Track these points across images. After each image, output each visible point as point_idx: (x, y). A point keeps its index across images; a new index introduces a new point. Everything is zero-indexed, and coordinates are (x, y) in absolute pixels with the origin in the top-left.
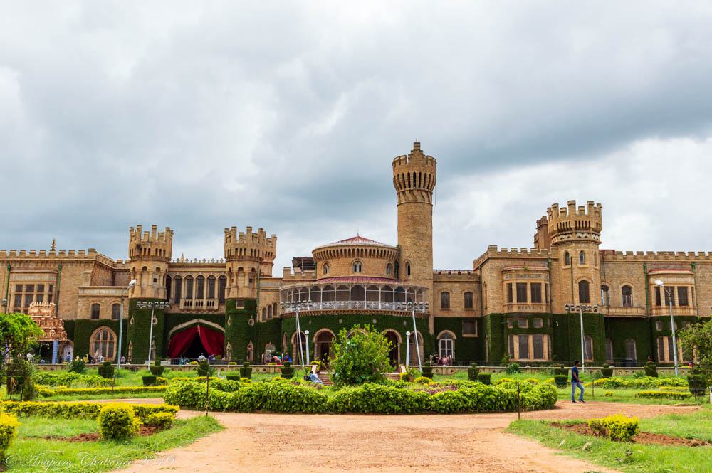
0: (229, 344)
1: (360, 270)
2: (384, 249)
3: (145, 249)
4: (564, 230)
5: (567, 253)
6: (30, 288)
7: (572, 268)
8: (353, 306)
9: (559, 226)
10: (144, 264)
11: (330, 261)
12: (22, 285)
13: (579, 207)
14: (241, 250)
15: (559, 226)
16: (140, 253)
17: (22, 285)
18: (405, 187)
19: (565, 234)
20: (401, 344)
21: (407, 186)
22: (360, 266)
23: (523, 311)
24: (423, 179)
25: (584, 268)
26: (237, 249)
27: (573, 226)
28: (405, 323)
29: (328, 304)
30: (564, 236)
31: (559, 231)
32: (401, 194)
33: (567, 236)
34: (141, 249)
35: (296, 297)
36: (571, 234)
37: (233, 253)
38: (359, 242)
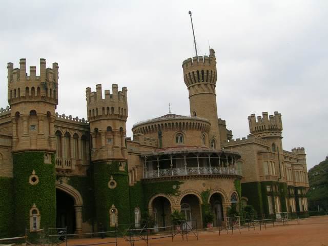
0: (113, 206)
1: (181, 141)
2: (142, 127)
3: (51, 89)
4: (273, 129)
5: (273, 145)
7: (278, 154)
8: (162, 174)
9: (270, 127)
10: (31, 107)
11: (185, 132)
13: (270, 116)
14: (122, 109)
15: (270, 127)
16: (47, 93)
18: (207, 81)
19: (273, 132)
20: (202, 205)
21: (209, 80)
22: (181, 138)
23: (268, 180)
24: (213, 76)
25: (274, 154)
26: (103, 108)
27: (267, 128)
28: (90, 189)
29: (165, 172)
30: (272, 133)
31: (269, 129)
32: (203, 86)
33: (274, 133)
34: (46, 89)
35: (155, 164)
36: (276, 132)
37: (100, 112)
38: (172, 118)
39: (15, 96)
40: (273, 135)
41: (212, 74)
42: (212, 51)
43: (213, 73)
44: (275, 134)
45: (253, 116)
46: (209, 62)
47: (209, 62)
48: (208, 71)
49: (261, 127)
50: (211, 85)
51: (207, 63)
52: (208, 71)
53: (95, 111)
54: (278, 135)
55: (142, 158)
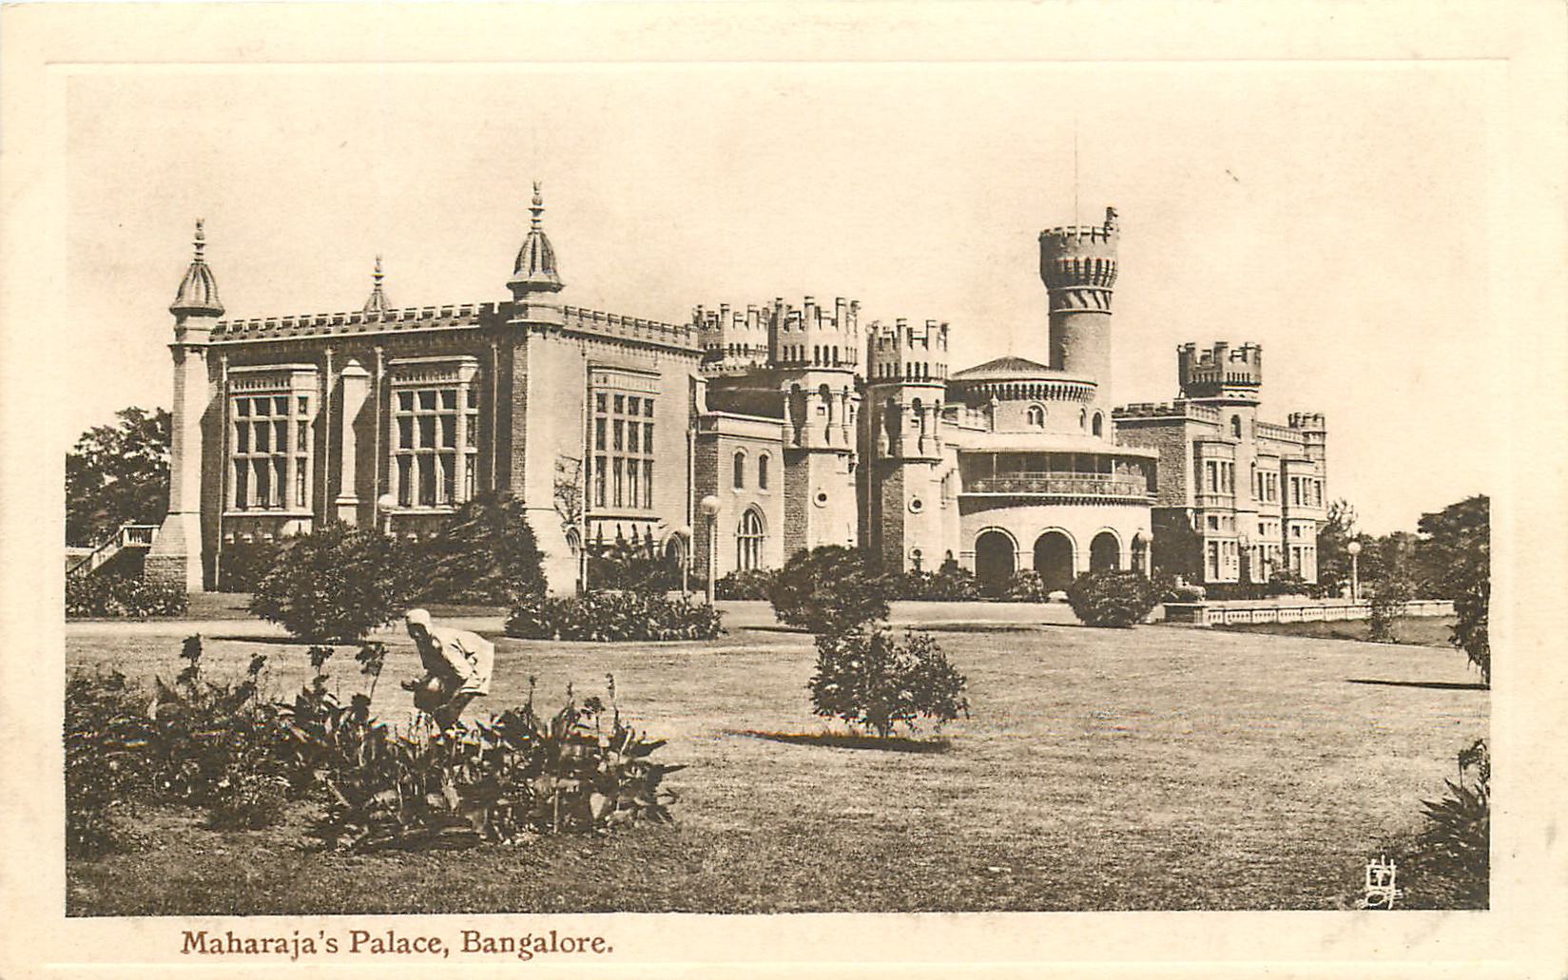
6: (634, 401)
12: (623, 397)
17: (623, 397)
39: (794, 357)
40: (1237, 397)
41: (1107, 269)
42: (1110, 212)
43: (1111, 267)
44: (1242, 396)
45: (1190, 348)
46: (1105, 240)
47: (1105, 240)
48: (1099, 261)
49: (1209, 378)
50: (1104, 292)
51: (1099, 239)
52: (1099, 261)
53: (893, 369)
54: (1249, 396)
55: (961, 455)
